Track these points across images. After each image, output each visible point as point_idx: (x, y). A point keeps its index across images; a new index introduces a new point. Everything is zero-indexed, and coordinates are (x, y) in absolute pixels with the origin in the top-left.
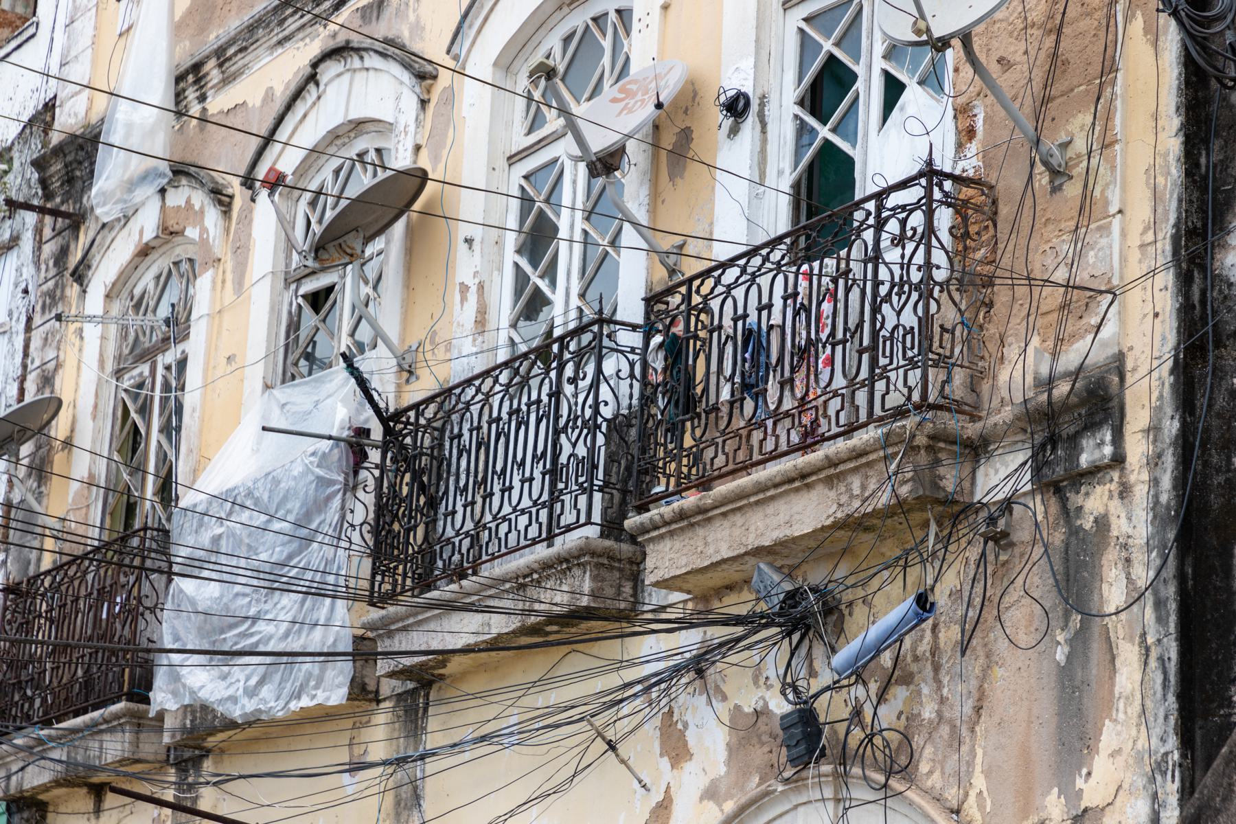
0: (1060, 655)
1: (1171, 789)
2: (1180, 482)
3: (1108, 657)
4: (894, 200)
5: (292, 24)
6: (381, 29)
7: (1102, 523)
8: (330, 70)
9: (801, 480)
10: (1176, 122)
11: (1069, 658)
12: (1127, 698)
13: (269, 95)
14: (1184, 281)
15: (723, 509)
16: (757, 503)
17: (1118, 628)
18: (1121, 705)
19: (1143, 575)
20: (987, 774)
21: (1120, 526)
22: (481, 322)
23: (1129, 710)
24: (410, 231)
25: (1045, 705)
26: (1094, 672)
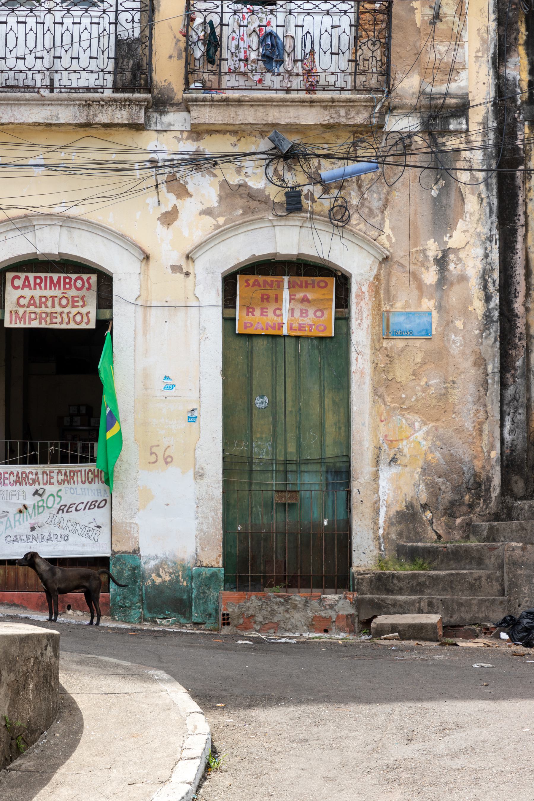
0: (434, 193)
3: (460, 198)
11: (438, 195)
12: (471, 214)
15: (253, 103)
16: (275, 106)
18: (468, 215)
20: (393, 229)
23: (472, 218)
26: (453, 202)
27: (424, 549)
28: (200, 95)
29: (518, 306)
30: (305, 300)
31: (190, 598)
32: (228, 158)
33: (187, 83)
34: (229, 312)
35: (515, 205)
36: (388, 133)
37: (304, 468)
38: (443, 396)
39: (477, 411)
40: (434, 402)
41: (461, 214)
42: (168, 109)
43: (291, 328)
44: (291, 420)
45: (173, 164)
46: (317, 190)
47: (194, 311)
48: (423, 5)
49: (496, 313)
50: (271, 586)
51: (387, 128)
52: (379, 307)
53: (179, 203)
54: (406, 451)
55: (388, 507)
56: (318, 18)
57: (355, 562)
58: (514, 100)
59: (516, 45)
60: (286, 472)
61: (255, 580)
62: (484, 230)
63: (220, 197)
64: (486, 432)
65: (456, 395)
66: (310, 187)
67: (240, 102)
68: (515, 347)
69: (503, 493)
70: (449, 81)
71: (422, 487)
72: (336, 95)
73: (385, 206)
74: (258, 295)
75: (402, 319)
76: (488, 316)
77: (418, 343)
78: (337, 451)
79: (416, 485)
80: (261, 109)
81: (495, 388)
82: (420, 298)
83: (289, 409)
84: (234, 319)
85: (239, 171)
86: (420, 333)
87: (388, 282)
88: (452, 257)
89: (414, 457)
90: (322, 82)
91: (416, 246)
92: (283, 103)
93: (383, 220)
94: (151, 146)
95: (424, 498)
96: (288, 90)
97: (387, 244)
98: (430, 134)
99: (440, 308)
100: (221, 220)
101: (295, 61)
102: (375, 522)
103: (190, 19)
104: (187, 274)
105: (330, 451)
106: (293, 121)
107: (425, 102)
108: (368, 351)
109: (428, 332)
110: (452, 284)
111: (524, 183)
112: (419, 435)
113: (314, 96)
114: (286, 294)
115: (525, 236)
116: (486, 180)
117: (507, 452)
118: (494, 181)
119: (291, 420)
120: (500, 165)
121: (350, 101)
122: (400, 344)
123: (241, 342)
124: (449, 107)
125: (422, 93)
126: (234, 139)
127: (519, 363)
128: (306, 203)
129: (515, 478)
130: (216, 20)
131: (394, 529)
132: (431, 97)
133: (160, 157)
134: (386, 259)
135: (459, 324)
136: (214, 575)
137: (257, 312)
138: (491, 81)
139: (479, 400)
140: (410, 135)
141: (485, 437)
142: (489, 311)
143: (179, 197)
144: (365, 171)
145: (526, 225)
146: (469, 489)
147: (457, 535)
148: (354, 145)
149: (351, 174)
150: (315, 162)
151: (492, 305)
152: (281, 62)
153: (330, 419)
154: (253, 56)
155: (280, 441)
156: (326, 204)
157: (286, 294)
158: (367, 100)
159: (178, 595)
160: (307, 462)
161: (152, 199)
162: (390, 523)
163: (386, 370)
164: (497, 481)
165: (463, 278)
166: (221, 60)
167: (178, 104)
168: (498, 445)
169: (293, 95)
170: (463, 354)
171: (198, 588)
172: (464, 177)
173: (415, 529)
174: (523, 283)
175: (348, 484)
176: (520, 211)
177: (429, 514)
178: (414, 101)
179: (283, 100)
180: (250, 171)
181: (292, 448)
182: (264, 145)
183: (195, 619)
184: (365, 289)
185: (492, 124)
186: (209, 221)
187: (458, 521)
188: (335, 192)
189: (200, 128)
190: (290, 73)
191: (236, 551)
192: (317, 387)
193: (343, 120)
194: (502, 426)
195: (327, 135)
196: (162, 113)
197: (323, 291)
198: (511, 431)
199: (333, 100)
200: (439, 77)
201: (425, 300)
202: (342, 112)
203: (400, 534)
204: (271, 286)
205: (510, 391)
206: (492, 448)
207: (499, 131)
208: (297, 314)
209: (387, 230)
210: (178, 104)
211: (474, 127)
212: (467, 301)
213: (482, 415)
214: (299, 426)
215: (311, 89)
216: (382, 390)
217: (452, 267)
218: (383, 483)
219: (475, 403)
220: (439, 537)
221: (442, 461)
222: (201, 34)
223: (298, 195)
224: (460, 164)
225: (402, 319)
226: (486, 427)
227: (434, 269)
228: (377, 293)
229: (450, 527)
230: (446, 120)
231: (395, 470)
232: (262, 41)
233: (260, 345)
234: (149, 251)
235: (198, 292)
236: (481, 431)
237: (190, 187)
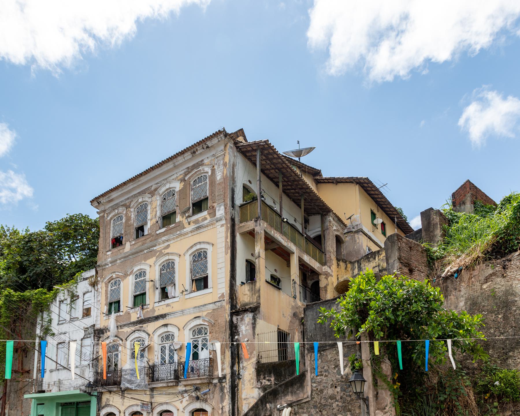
2: (231, 384)
4: (206, 359)
5: (130, 326)
6: (142, 329)
7: (224, 386)
8: (137, 331)
9: (198, 379)
13: (127, 331)
14: (231, 370)
17: (226, 394)
19: (228, 390)
21: (226, 386)
22: (158, 358)
24: (148, 348)
25: (220, 398)
35: (235, 396)
58: (236, 374)
126: (190, 386)
140: (216, 383)
176: (236, 397)
186: (187, 402)
230: (222, 380)
234: (179, 408)
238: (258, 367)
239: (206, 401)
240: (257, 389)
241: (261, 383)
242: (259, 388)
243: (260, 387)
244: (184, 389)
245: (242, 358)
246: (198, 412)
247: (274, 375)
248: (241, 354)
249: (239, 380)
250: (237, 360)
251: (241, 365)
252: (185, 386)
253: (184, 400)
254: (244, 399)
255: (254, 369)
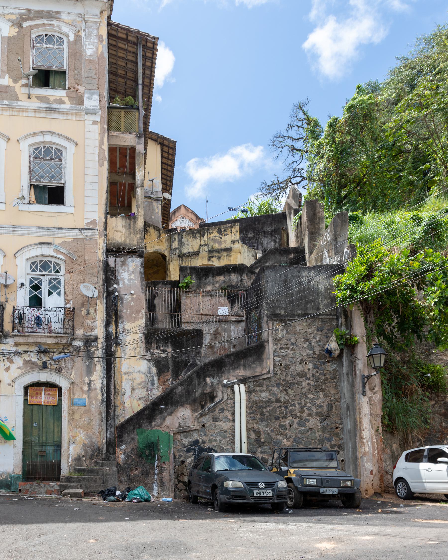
0: (87, 364)
1: (105, 380)
10: (105, 314)
20: (75, 374)
27: (82, 469)
28: (17, 334)
29: (112, 397)
30: (49, 394)
31: (11, 484)
32: (26, 352)
33: (13, 329)
34: (26, 398)
36: (73, 346)
37: (48, 444)
38: (89, 423)
39: (99, 428)
40: (87, 425)
41: (95, 370)
42: (8, 337)
43: (44, 403)
44: (44, 430)
45: (9, 354)
46: (52, 362)
47: (14, 397)
48: (84, 310)
49: (105, 399)
50: (36, 480)
51: (73, 345)
52: (70, 397)
53: (11, 365)
54: (78, 440)
55: (72, 456)
56: (52, 312)
57: (62, 473)
58: (111, 337)
59: (112, 322)
60: (42, 445)
61: (32, 478)
62: (102, 375)
63: (23, 364)
64: (102, 434)
65: (93, 423)
66: (50, 361)
67: (29, 336)
68: (111, 409)
69: (106, 453)
70: (92, 332)
71: (82, 450)
72: (58, 335)
73: (73, 367)
74: (35, 393)
75: (77, 400)
76: (103, 400)
77: (82, 408)
78: (58, 440)
79: (81, 450)
80: (35, 338)
81: (105, 421)
82: (83, 394)
83: (44, 427)
84: (27, 400)
85: (29, 356)
86: (82, 405)
87: (73, 389)
88: (92, 382)
89: (80, 442)
90: (53, 331)
91: (81, 379)
92: (42, 336)
93: (72, 371)
94: (2, 348)
95: (83, 454)
96: (45, 333)
97: (73, 378)
98: (86, 347)
99: (88, 397)
100: (23, 370)
101: (45, 324)
102: (68, 461)
103: (14, 312)
104: (13, 386)
105: (56, 439)
106: (44, 342)
107: (84, 337)
108: (67, 410)
109: (85, 404)
110: (92, 391)
111: (114, 361)
112: (82, 435)
113: (51, 335)
114: (43, 393)
115: (114, 377)
116: (102, 360)
117: (108, 440)
118: (105, 361)
119: (44, 430)
120: (106, 356)
121: (62, 336)
122: (76, 408)
123: (29, 407)
124: (91, 339)
125: (84, 335)
126: (28, 347)
127: (112, 414)
128: (49, 366)
129: (110, 448)
130: (22, 312)
131: (74, 463)
132: (86, 336)
133: (5, 351)
134: (73, 383)
135: (94, 402)
136: (19, 477)
137: (34, 398)
138: (104, 332)
139: (100, 425)
140: (80, 347)
141: (101, 436)
142: (103, 398)
143: (11, 363)
144: (66, 357)
145: (114, 374)
146: (96, 451)
147: (93, 465)
148: (64, 349)
149: (62, 358)
150: (52, 354)
151: (104, 397)
152: (41, 325)
153: (56, 430)
154: (33, 323)
155: (41, 436)
156: (55, 366)
157: (43, 393)
158: (66, 336)
159: (7, 483)
160: (49, 443)
161: (2, 364)
162: (73, 461)
163: (72, 416)
164: (105, 449)
165: (95, 389)
166: (23, 323)
167: (11, 336)
168: (105, 438)
169: (46, 334)
170: (95, 411)
171: (14, 481)
172: (96, 359)
173: (80, 463)
174: (113, 391)
175: (61, 450)
177: (84, 459)
178: (81, 337)
179: (42, 336)
180: (32, 356)
181: (44, 438)
182: (37, 349)
183: (12, 490)
184: (66, 391)
185: (105, 344)
186: (20, 371)
187: (93, 461)
188: (57, 363)
189: (17, 343)
190: (44, 328)
191: (26, 469)
192: (52, 420)
193: (60, 342)
194: (107, 433)
195: (56, 346)
196: (6, 339)
197: (55, 392)
198: (109, 434)
199: (56, 336)
200: (89, 330)
201: (84, 395)
202: (59, 340)
203: (76, 465)
204: (39, 390)
205: (109, 422)
206: (104, 439)
207: (106, 346)
208: (46, 399)
209: (73, 374)
210: (11, 336)
211: (99, 346)
212: (97, 396)
213: (101, 429)
214: (46, 432)
215: (50, 333)
216: (71, 421)
217: (92, 385)
218: (71, 449)
219: (99, 426)
220: (87, 465)
221: (89, 443)
222: (17, 316)
223: (46, 363)
224: (95, 356)
225: (77, 400)
226: (102, 433)
227: (87, 386)
228: (70, 393)
229: (91, 463)
230: (91, 342)
231: (74, 445)
232: (36, 319)
233: (35, 408)
235: (16, 391)
236: (100, 434)
237: (14, 361)
238: (148, 331)
239: (59, 370)
240: (146, 362)
241: (152, 354)
242: (149, 360)
243: (150, 358)
244: (14, 349)
245: (121, 317)
246: (36, 388)
247: (172, 346)
248: (121, 311)
249: (116, 346)
250: (114, 317)
251: (120, 326)
252: (16, 344)
253: (14, 367)
254: (125, 373)
255: (142, 334)
